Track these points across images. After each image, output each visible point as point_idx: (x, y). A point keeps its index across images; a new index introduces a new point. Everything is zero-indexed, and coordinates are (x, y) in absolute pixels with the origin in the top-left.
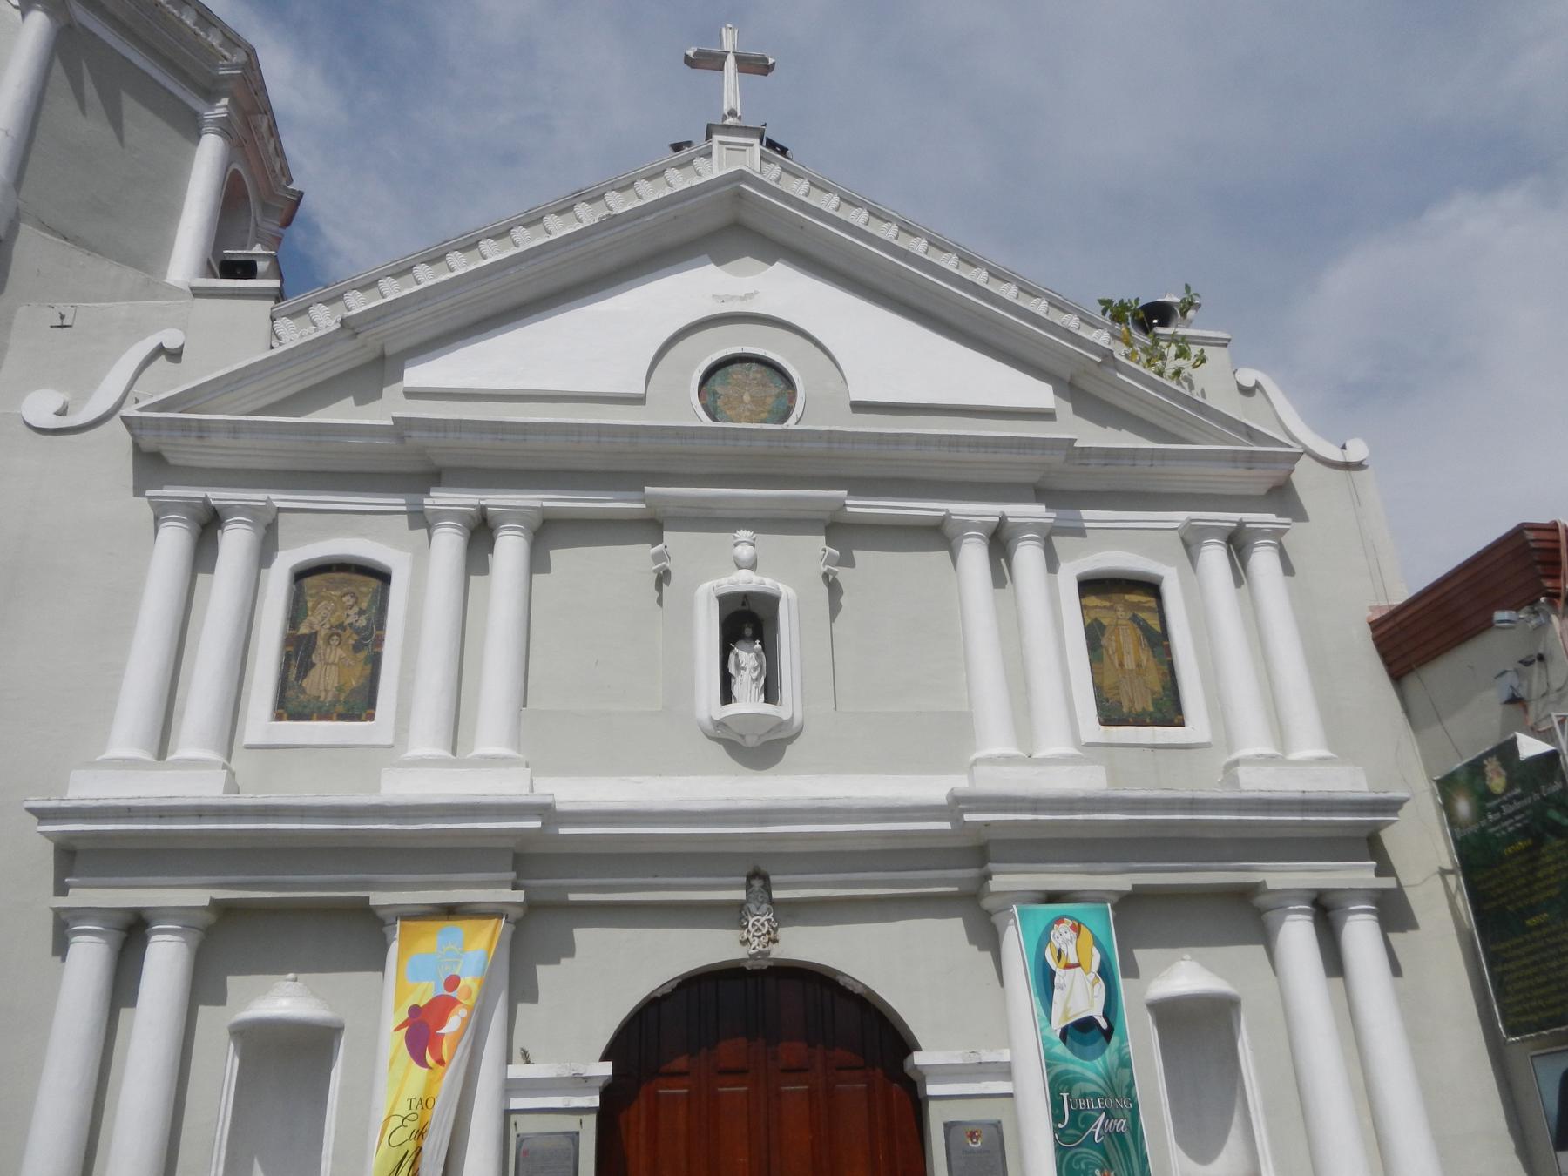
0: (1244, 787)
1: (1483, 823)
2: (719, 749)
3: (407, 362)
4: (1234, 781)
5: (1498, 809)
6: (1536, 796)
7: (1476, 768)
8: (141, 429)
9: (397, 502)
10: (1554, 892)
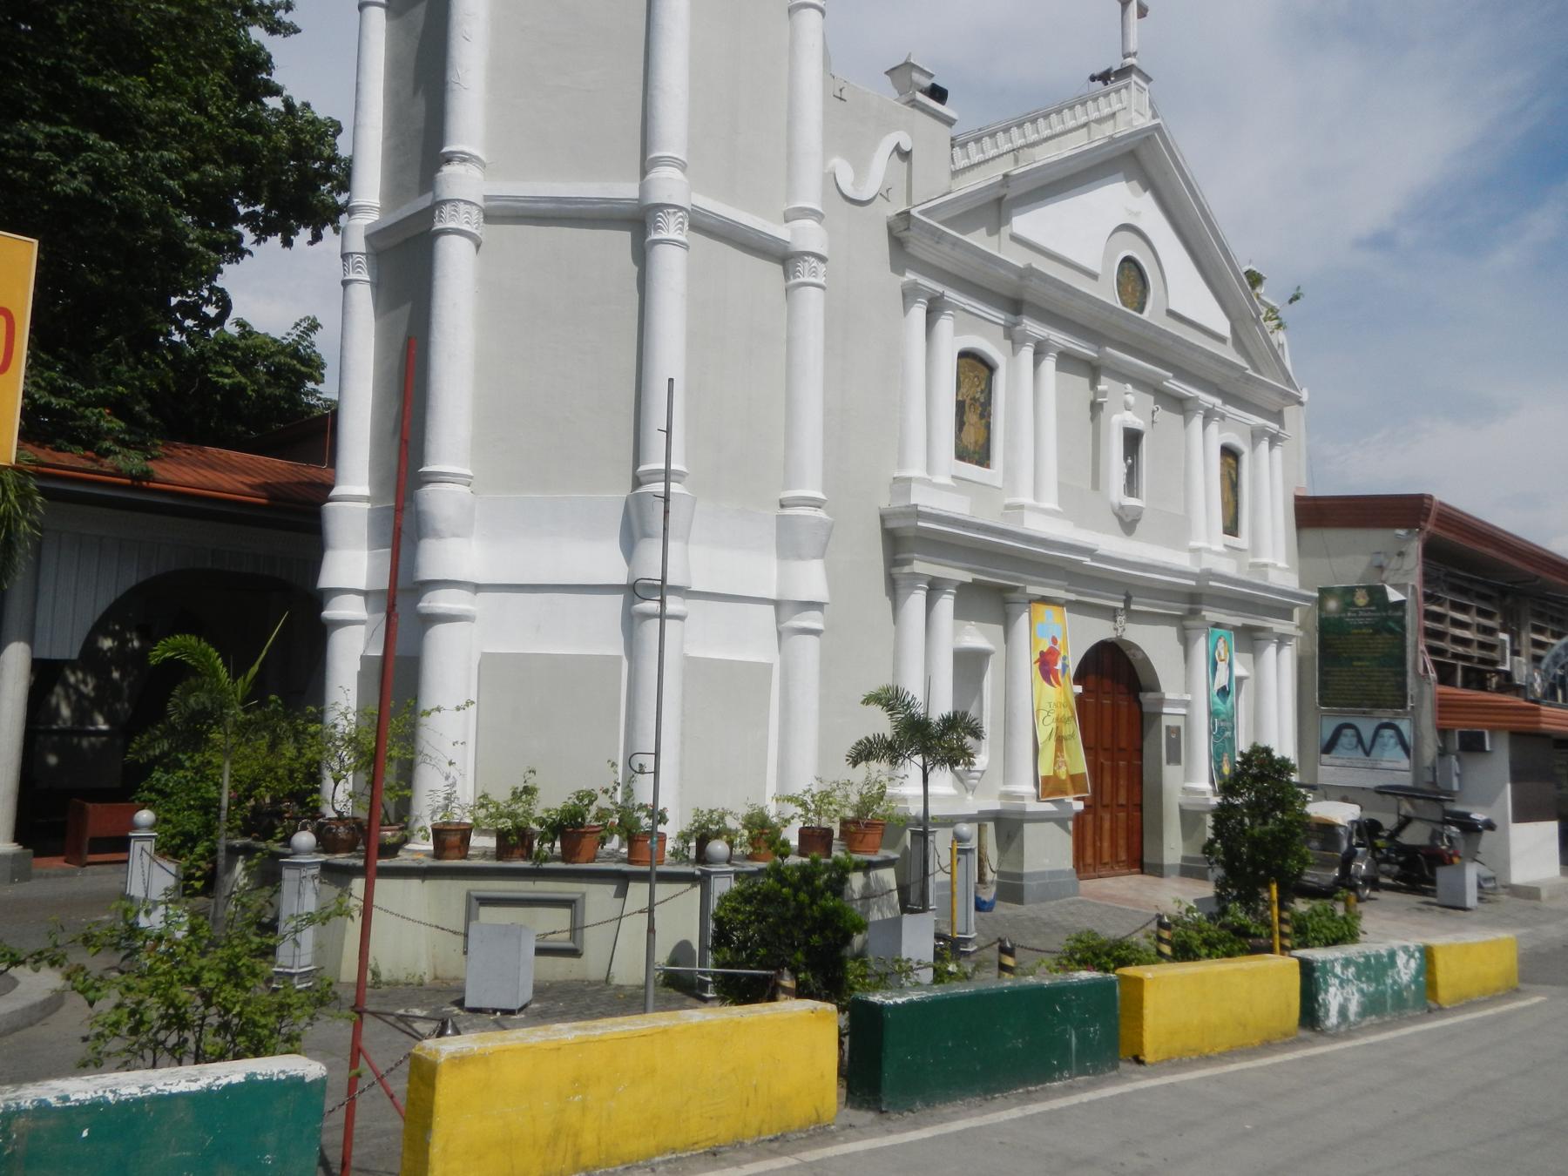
0: (1270, 580)
1: (1343, 615)
2: (1116, 521)
3: (1014, 211)
4: (1265, 576)
5: (1357, 612)
6: (1384, 614)
7: (1350, 591)
9: (999, 316)
10: (1377, 655)
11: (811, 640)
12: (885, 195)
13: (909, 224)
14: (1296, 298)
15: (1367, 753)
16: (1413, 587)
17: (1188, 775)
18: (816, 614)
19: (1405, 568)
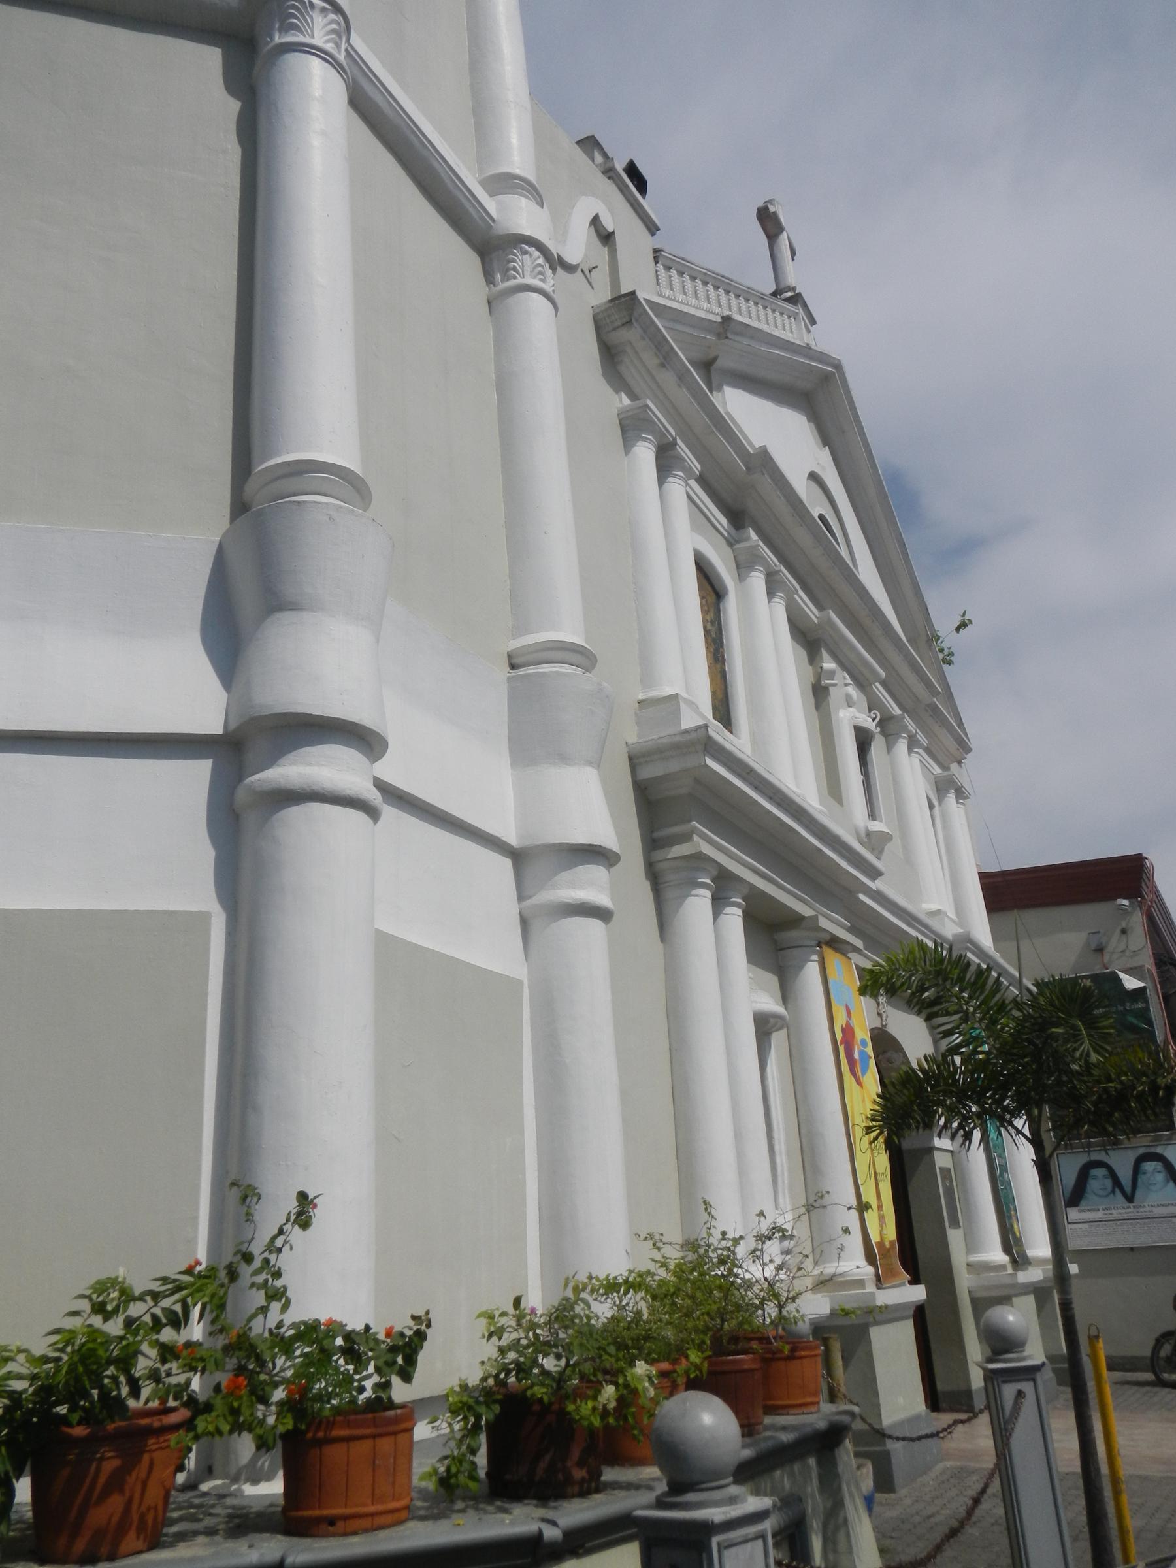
8: (637, 321)
11: (595, 926)
12: (587, 272)
13: (631, 315)
14: (963, 625)
15: (1130, 1199)
16: (1148, 969)
17: (972, 1245)
18: (597, 872)
19: (1132, 948)
